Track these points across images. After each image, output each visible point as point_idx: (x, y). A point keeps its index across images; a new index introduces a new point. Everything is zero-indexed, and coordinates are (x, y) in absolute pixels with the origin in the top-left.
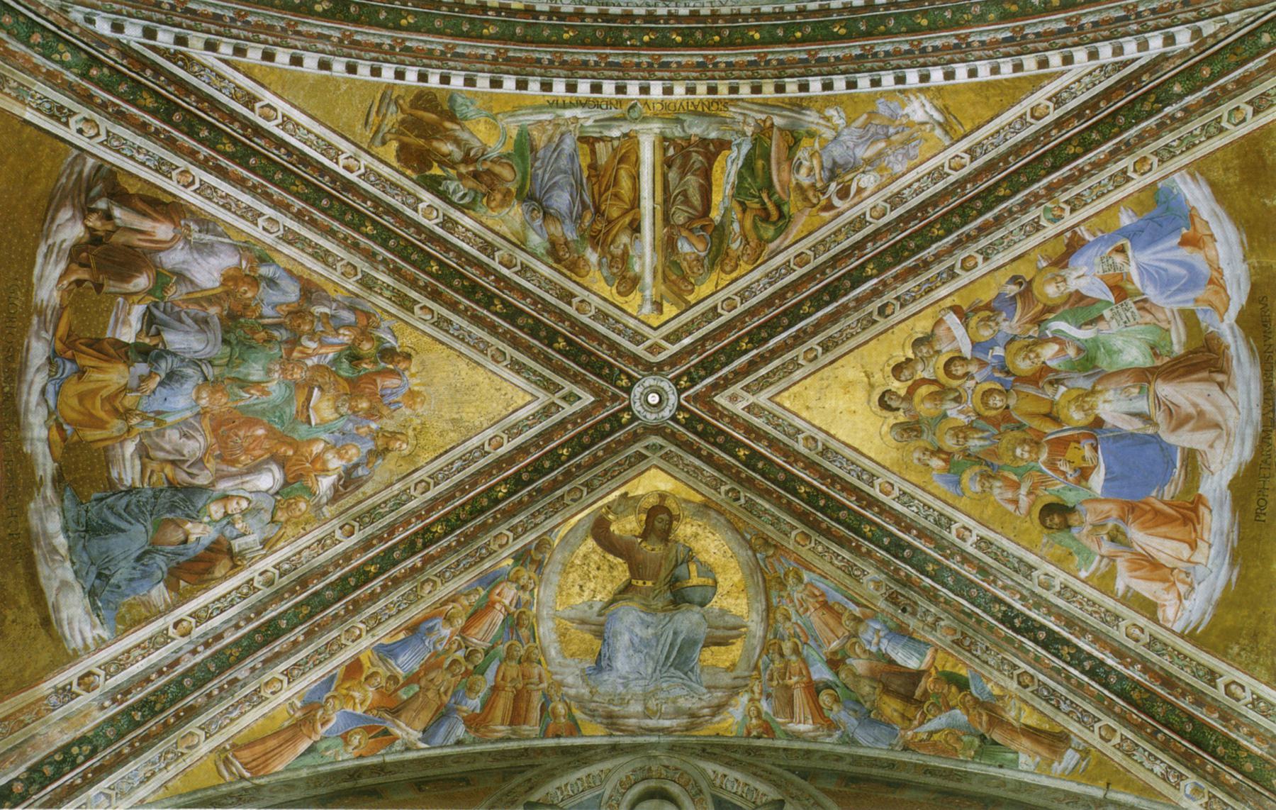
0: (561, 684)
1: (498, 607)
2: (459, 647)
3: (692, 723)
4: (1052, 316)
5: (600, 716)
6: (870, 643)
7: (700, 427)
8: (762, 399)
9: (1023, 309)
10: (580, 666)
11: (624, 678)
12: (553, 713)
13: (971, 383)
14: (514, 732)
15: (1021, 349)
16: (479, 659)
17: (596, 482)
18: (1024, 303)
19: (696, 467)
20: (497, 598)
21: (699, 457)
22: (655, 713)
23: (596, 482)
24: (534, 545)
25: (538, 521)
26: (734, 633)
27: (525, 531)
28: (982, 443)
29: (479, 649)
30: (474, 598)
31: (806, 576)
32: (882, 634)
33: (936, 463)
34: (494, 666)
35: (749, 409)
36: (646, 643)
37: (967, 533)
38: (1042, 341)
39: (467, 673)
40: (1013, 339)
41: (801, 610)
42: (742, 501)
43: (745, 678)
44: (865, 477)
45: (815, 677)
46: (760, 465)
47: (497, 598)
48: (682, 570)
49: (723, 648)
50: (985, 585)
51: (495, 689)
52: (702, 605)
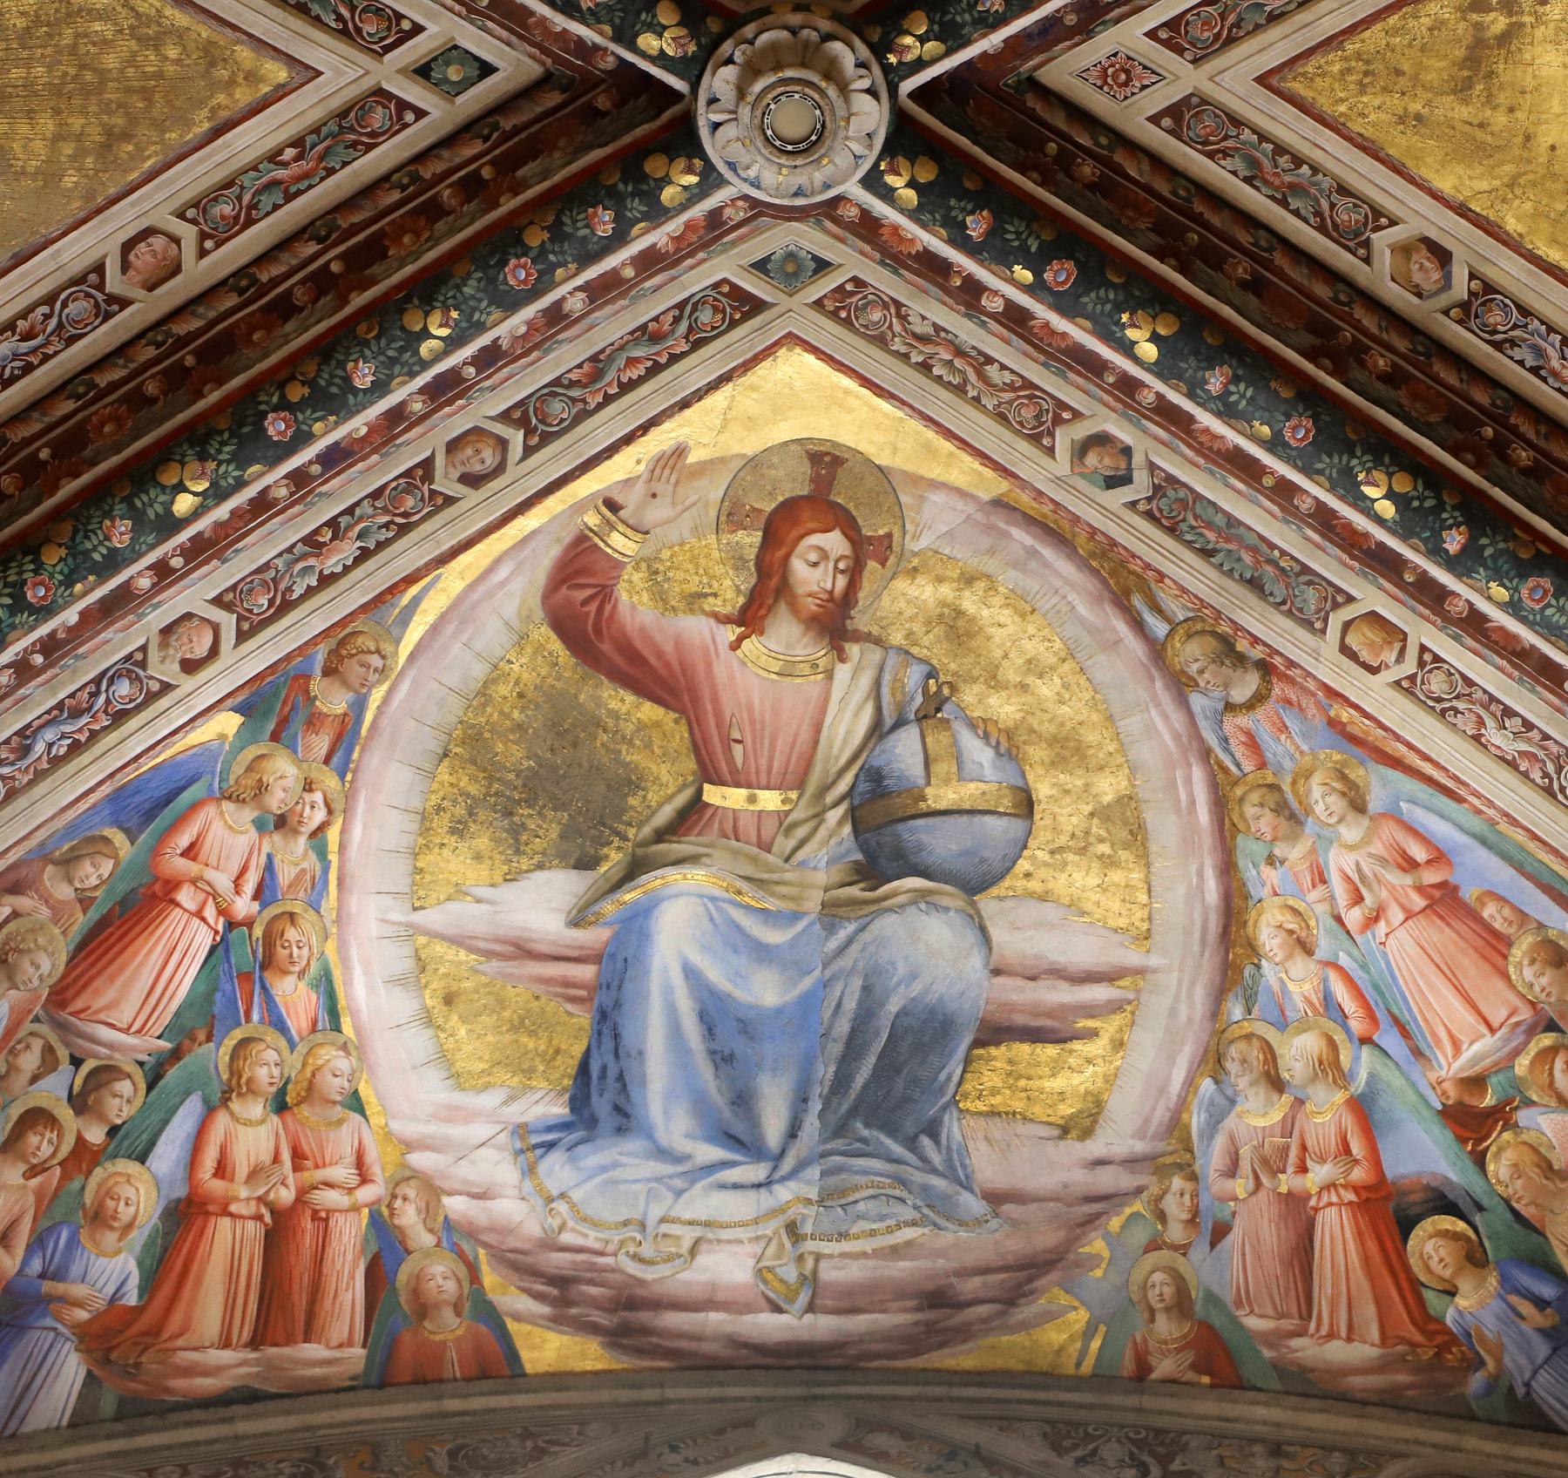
1: (186, 897)
2: (49, 1062)
3: (930, 1328)
16: (124, 1099)
17: (557, 407)
23: (557, 407)
24: (321, 654)
25: (332, 564)
26: (1098, 993)
29: (120, 1059)
30: (93, 873)
31: (1381, 785)
35: (1177, 115)
41: (1353, 917)
42: (1140, 486)
47: (182, 865)
48: (905, 751)
49: (1051, 1050)
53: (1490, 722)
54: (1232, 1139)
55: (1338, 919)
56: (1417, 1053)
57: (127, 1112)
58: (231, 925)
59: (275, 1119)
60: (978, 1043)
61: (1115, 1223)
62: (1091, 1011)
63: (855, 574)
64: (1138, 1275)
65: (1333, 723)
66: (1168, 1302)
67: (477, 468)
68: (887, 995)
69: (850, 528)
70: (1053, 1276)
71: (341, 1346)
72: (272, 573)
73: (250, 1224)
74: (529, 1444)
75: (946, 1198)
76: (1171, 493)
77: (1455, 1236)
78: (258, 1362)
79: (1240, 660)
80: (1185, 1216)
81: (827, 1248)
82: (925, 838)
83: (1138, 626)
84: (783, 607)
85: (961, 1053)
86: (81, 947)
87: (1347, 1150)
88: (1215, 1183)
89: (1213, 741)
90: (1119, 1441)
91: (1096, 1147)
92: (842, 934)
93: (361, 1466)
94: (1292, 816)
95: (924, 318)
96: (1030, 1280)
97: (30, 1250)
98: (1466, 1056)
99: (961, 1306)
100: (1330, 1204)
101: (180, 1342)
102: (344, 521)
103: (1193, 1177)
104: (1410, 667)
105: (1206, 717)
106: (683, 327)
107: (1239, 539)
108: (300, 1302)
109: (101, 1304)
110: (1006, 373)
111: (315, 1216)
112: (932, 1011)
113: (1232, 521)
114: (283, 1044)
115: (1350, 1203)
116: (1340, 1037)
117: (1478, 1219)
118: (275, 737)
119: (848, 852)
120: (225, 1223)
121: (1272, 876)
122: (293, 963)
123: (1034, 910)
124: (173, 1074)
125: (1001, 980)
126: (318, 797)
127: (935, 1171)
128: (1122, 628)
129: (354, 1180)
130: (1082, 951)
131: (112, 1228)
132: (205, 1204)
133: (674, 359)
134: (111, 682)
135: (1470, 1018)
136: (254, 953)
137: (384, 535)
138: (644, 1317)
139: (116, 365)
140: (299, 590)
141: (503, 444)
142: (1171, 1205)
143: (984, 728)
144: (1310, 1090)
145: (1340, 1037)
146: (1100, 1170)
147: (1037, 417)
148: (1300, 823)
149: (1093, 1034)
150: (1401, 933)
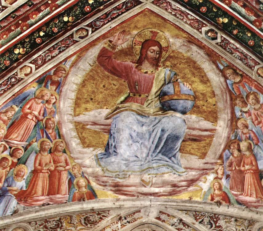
0: (81, 166)
1: (30, 117)
3: (174, 191)
5: (110, 186)
10: (94, 153)
11: (126, 160)
12: (78, 185)
14: (51, 200)
16: (21, 153)
19: (182, 12)
20: (28, 111)
22: (148, 184)
24: (52, 71)
25: (54, 54)
27: (44, 62)
29: (20, 147)
34: (32, 157)
36: (141, 136)
39: (14, 165)
42: (219, 40)
43: (212, 164)
51: (35, 172)
57: (21, 156)
58: (39, 121)
59: (49, 155)
62: (205, 136)
66: (218, 188)
67: (82, 35)
71: (64, 195)
72: (41, 57)
73: (46, 174)
74: (99, 216)
76: (225, 41)
78: (49, 198)
79: (237, 74)
80: (221, 173)
86: (9, 128)
90: (208, 217)
93: (68, 222)
95: (175, 6)
97: (4, 182)
99: (179, 187)
100: (248, 173)
101: (34, 196)
102: (56, 46)
105: (230, 84)
106: (124, 7)
108: (56, 187)
109: (19, 191)
110: (192, 17)
111: (58, 172)
114: (49, 141)
115: (252, 173)
118: (45, 86)
119: (159, 105)
120: (41, 174)
122: (51, 127)
124: (29, 148)
126: (54, 97)
129: (65, 165)
131: (20, 177)
132: (37, 171)
133: (122, 13)
134: (11, 79)
136: (43, 125)
137: (63, 49)
138: (120, 188)
139: (5, 22)
140: (47, 60)
141: (87, 31)
146: (206, 165)
147: (198, 25)
149: (205, 140)
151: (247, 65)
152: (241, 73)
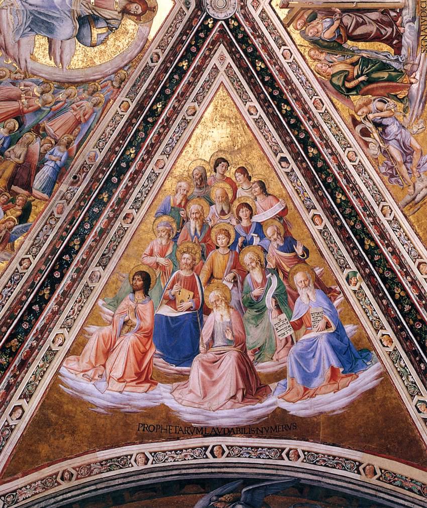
4: (281, 275)
6: (52, 154)
7: (202, 35)
8: (222, 77)
9: (285, 257)
13: (234, 222)
15: (259, 257)
18: (289, 258)
21: (181, 34)
26: (58, 60)
28: (192, 230)
31: (99, 109)
32: (58, 162)
33: (179, 198)
37: (129, 221)
38: (264, 270)
40: (265, 252)
41: (74, 106)
42: (151, 64)
44: (168, 149)
45: (27, 116)
46: (176, 77)
50: (93, 234)
52: (79, 37)
53: (111, 128)
54: (31, 85)
55: (74, 103)
56: (49, 119)
60: (48, 38)
61: (15, 65)
63: (134, 15)
64: (5, 69)
65: (110, 100)
68: (57, 21)
69: (143, 13)
70: (4, 53)
75: (18, 33)
77: (15, 127)
81: (9, 11)
82: (86, 28)
83: (126, 65)
84: (128, 2)
85: (46, 35)
87: (30, 107)
88: (22, 83)
89: (106, 79)
91: (29, 60)
92: (67, 13)
94: (92, 94)
96: (3, 49)
98: (49, 127)
103: (24, 79)
104: (120, 113)
107: (142, 82)
112: (54, 30)
113: (145, 81)
116: (51, 104)
117: (18, 132)
121: (81, 90)
123: (73, 47)
125: (60, 42)
127: (23, 31)
128: (126, 62)
130: (66, 58)
135: (56, 128)
142: (18, 75)
143: (107, 38)
144: (41, 99)
145: (51, 104)
148: (91, 96)
149: (51, 60)
150: (72, 114)
151: (129, 91)
152: (122, 86)
